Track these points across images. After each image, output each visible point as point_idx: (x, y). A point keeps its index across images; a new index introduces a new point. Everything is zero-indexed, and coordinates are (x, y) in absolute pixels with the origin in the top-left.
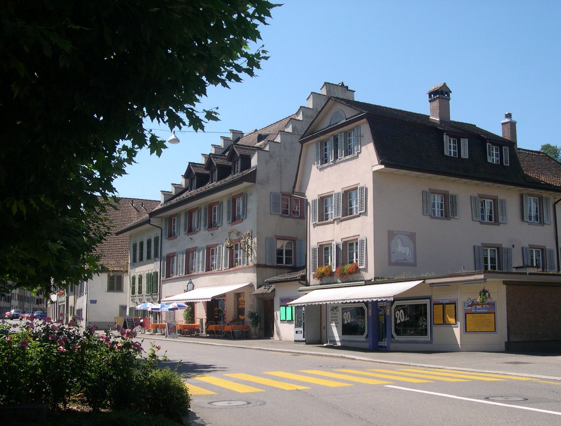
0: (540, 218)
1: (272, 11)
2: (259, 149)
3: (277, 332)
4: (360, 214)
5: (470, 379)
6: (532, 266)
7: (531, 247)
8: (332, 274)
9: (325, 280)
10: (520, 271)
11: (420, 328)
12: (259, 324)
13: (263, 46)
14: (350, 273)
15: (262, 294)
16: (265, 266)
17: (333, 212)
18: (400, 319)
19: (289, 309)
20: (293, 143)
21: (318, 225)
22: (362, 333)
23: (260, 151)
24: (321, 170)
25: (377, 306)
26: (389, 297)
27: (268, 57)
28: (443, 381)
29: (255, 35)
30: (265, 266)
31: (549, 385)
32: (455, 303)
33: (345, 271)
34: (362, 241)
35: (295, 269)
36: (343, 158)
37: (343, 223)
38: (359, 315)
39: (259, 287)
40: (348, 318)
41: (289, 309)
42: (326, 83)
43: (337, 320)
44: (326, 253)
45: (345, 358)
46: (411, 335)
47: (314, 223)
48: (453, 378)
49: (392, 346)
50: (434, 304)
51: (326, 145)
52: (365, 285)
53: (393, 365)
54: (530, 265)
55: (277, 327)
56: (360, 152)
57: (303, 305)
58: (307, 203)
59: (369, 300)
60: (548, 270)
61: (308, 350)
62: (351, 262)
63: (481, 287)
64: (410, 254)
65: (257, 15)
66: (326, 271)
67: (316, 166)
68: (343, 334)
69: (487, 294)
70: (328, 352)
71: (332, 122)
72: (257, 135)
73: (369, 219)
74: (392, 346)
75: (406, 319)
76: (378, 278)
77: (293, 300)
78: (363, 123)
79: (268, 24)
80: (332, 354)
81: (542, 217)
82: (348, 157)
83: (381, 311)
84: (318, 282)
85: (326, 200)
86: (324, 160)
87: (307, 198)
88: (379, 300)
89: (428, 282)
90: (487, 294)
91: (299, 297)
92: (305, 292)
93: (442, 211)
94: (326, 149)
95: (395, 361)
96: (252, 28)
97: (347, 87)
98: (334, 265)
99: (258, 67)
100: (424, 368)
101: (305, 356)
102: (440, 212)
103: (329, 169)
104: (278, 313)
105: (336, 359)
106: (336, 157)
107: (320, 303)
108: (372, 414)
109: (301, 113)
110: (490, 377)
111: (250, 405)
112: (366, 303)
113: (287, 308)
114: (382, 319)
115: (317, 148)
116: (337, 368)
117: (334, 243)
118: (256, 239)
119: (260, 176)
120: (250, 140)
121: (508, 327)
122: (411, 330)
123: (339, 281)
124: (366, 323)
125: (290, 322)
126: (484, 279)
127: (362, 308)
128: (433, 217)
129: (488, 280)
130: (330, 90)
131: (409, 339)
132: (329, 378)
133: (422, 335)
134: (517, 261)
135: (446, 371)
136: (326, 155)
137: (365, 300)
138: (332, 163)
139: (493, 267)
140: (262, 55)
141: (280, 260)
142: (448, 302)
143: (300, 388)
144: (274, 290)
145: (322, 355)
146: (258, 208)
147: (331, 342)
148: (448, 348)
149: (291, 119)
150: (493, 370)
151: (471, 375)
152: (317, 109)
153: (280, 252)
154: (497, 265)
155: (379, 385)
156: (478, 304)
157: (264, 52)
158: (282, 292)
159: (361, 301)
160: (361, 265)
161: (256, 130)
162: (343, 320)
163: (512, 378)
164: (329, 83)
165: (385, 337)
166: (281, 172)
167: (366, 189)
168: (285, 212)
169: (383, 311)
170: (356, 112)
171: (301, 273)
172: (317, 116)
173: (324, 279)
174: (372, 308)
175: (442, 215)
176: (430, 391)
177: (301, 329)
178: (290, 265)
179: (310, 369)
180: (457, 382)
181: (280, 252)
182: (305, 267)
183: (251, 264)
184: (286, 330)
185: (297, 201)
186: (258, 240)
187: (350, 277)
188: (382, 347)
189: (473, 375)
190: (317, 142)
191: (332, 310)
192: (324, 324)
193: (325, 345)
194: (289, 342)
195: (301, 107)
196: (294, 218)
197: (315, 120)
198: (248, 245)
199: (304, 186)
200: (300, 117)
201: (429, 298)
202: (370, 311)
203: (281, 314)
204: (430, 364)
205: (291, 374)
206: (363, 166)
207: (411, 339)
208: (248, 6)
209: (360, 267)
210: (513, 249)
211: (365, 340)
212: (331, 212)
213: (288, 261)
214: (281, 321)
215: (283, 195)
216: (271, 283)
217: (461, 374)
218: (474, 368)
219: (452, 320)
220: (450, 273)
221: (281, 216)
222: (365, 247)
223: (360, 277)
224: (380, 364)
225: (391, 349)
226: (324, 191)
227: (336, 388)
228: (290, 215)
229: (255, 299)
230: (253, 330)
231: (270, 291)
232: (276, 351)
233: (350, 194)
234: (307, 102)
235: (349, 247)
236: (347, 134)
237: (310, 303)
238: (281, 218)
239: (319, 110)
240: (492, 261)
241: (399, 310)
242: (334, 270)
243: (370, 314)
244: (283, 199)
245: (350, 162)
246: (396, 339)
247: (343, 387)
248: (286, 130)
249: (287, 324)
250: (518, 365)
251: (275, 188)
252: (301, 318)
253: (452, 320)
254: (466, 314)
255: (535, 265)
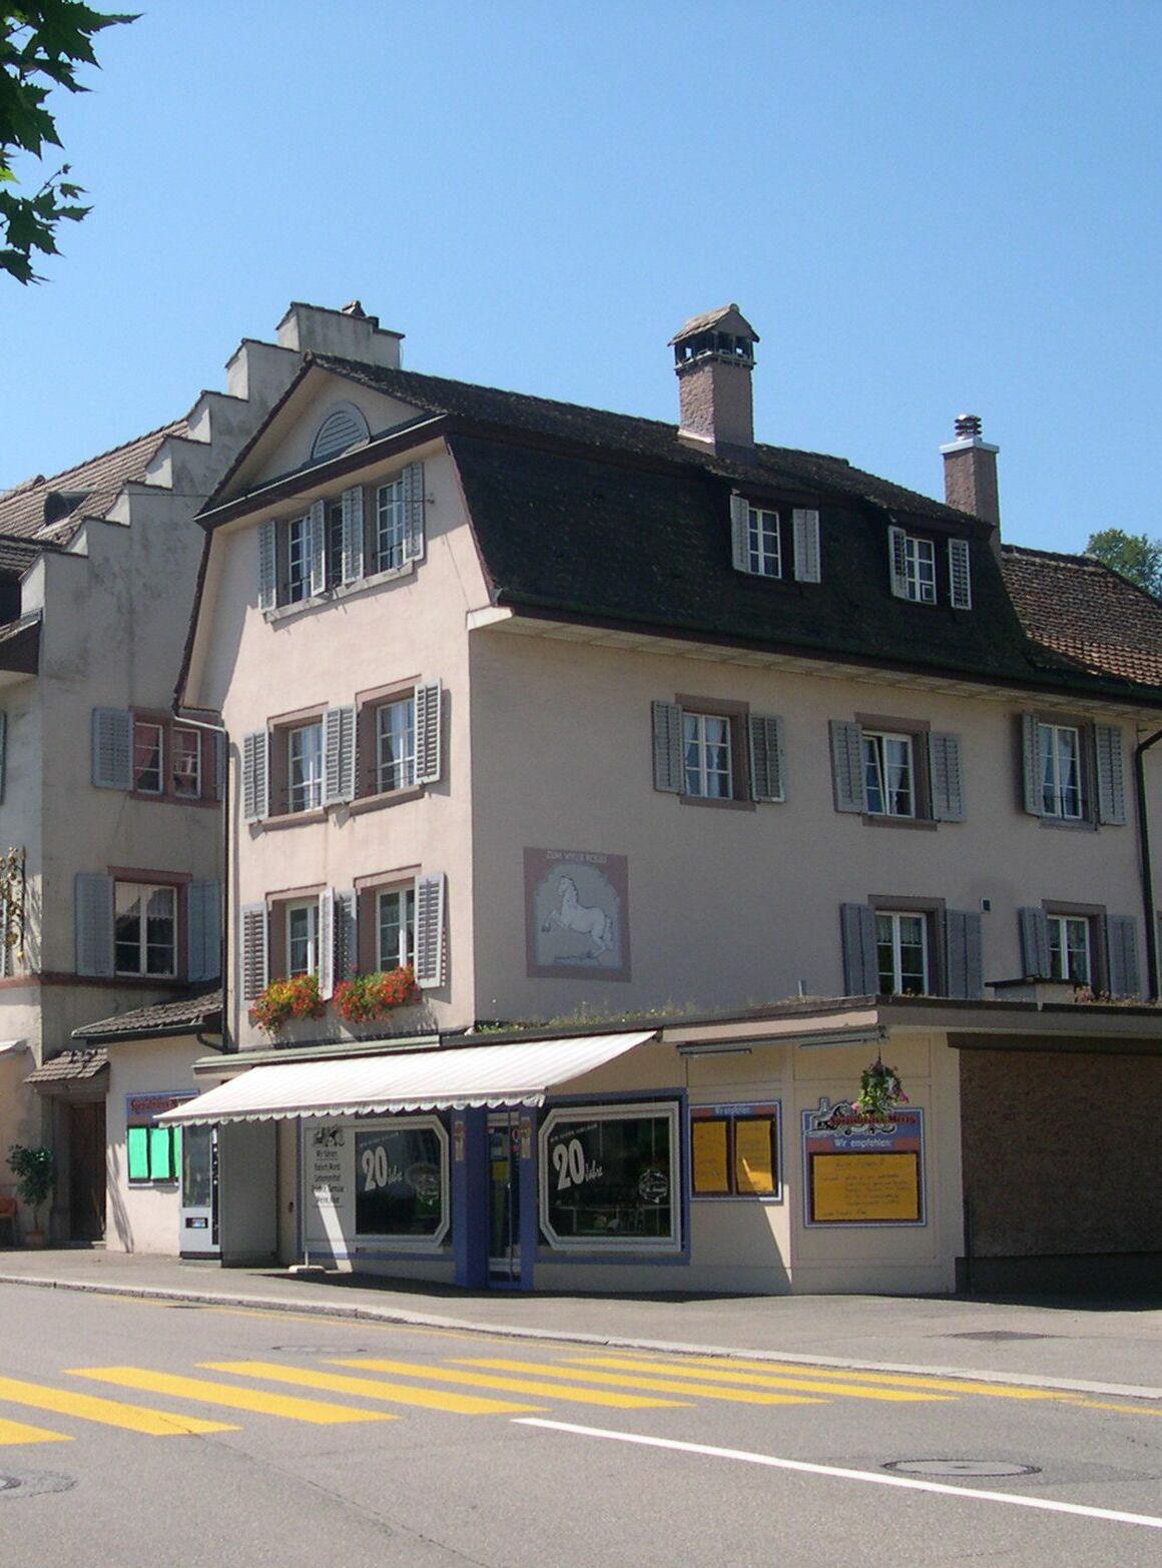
0: (1085, 803)
1: (98, 40)
2: (51, 547)
3: (118, 1223)
4: (424, 786)
5: (828, 1396)
6: (1055, 979)
7: (1053, 908)
8: (318, 1009)
9: (292, 1033)
10: (1011, 997)
11: (643, 1208)
12: (50, 1194)
13: (66, 169)
14: (387, 1005)
15: (63, 1082)
16: (73, 980)
17: (323, 780)
18: (568, 1174)
19: (160, 1137)
20: (176, 526)
21: (268, 828)
22: (430, 1226)
23: (53, 556)
24: (278, 624)
25: (486, 1128)
26: (530, 1094)
27: (85, 211)
28: (726, 1404)
29: (37, 130)
30: (73, 980)
31: (1117, 1417)
32: (770, 1117)
33: (367, 997)
34: (430, 888)
35: (184, 990)
36: (361, 582)
37: (360, 819)
38: (418, 1159)
39: (50, 1055)
40: (380, 1173)
41: (160, 1137)
42: (296, 307)
43: (337, 1178)
44: (299, 932)
45: (365, 1316)
46: (611, 1232)
47: (254, 820)
48: (766, 1390)
49: (542, 1272)
50: (694, 1120)
51: (296, 535)
52: (442, 1049)
53: (544, 1345)
54: (1047, 974)
55: (117, 1204)
56: (424, 560)
57: (211, 1121)
58: (228, 749)
59: (455, 1104)
60: (1114, 995)
61: (230, 1290)
62: (391, 965)
63: (866, 1057)
64: (608, 936)
65: (42, 55)
66: (299, 996)
67: (259, 611)
68: (360, 1229)
69: (891, 1083)
70: (304, 1297)
71: (323, 447)
72: (42, 497)
73: (456, 807)
74: (542, 1272)
75: (592, 1176)
76: (490, 1024)
77: (175, 1104)
78: (434, 453)
79: (82, 89)
80: (319, 1304)
81: (1091, 798)
82: (377, 578)
83: (499, 1144)
84: (268, 1038)
85: (297, 738)
86: (291, 589)
87: (229, 727)
88: (493, 1104)
89: (673, 1036)
90: (891, 1083)
91: (200, 1093)
92: (219, 1076)
93: (723, 779)
94: (296, 550)
95: (553, 1327)
96: (26, 105)
97: (375, 321)
98: (325, 975)
99: (49, 247)
100: (657, 1356)
101: (222, 1310)
102: (716, 781)
103: (308, 622)
104: (121, 1152)
105: (333, 1323)
106: (334, 579)
107: (276, 1117)
108: (466, 1524)
109: (206, 415)
110: (901, 1388)
111: (18, 1491)
112: (446, 1117)
113: (156, 1133)
114: (502, 1173)
115: (264, 543)
116: (338, 1354)
117: (327, 894)
118: (38, 879)
119: (52, 648)
120: (19, 517)
121: (966, 1202)
122: (611, 1216)
123: (345, 1034)
124: (444, 1190)
125: (165, 1184)
126: (881, 1029)
127: (429, 1135)
128: (690, 798)
129: (894, 1030)
130: (311, 332)
131: (601, 1248)
132: (308, 1393)
133: (651, 1232)
134: (1000, 960)
135: (738, 1364)
136: (296, 570)
137: (442, 1106)
138: (319, 601)
139: (913, 984)
140: (62, 202)
141: (127, 957)
142: (745, 1112)
143: (201, 1427)
144: (106, 1067)
145: (282, 1308)
146: (47, 764)
147: (315, 1257)
148: (747, 1281)
149: (170, 440)
150: (914, 1360)
151: (832, 1381)
152: (263, 403)
153: (127, 928)
154: (925, 975)
155: (491, 1419)
156: (856, 1119)
157: (67, 190)
158: (135, 1073)
159: (426, 1107)
160: (427, 973)
161: (40, 480)
162: (360, 1179)
163: (983, 1390)
164: (307, 306)
165: (515, 1242)
166: (131, 633)
167: (446, 696)
168: (148, 781)
169: (507, 1145)
170: (407, 413)
171: (206, 1005)
172: (266, 425)
173: (289, 1027)
174: (467, 1132)
175: (723, 792)
176: (681, 1438)
177: (206, 1212)
178: (166, 975)
179: (238, 1359)
180: (779, 1407)
181: (127, 928)
182: (219, 983)
183: (19, 971)
184: (150, 1215)
185: (189, 738)
186: (46, 884)
187: (387, 1021)
188: (503, 1276)
189: (840, 1382)
190: (263, 524)
191: (319, 1141)
192: (288, 1195)
193: (293, 1269)
194: (160, 1258)
195: (205, 394)
196: (179, 801)
197: (255, 440)
198: (10, 904)
199: (217, 682)
200: (202, 432)
201: (678, 1096)
202: (459, 1145)
203: (131, 1154)
204: (679, 1340)
205: (167, 1377)
206: (431, 612)
207: (609, 1248)
208: (10, 21)
209: (424, 984)
210: (986, 918)
211: (440, 1251)
212: (317, 779)
213: (159, 959)
214: (131, 1181)
215: (138, 718)
216: (94, 1041)
217: (793, 1377)
218: (842, 1355)
219: (761, 1179)
220: (752, 1004)
221: (133, 794)
222: (441, 902)
223: (422, 1019)
224: (497, 1340)
225: (538, 1285)
226: (292, 702)
227: (334, 1429)
228: (165, 793)
229: (38, 1101)
230: (28, 1214)
231: (89, 1072)
232: (113, 1292)
233: (386, 714)
234: (228, 375)
235: (381, 911)
236: (375, 494)
237: (238, 1114)
238: (130, 803)
239: (272, 404)
240: (908, 959)
241: (567, 1143)
242: (327, 994)
243: (459, 1157)
244: (138, 732)
245: (384, 597)
246: (555, 1247)
247: (361, 1424)
248: (151, 479)
249: (155, 1193)
250: (1003, 1344)
251: (108, 691)
252: (203, 1170)
253: (761, 1179)
254: (811, 1156)
255: (1065, 975)
